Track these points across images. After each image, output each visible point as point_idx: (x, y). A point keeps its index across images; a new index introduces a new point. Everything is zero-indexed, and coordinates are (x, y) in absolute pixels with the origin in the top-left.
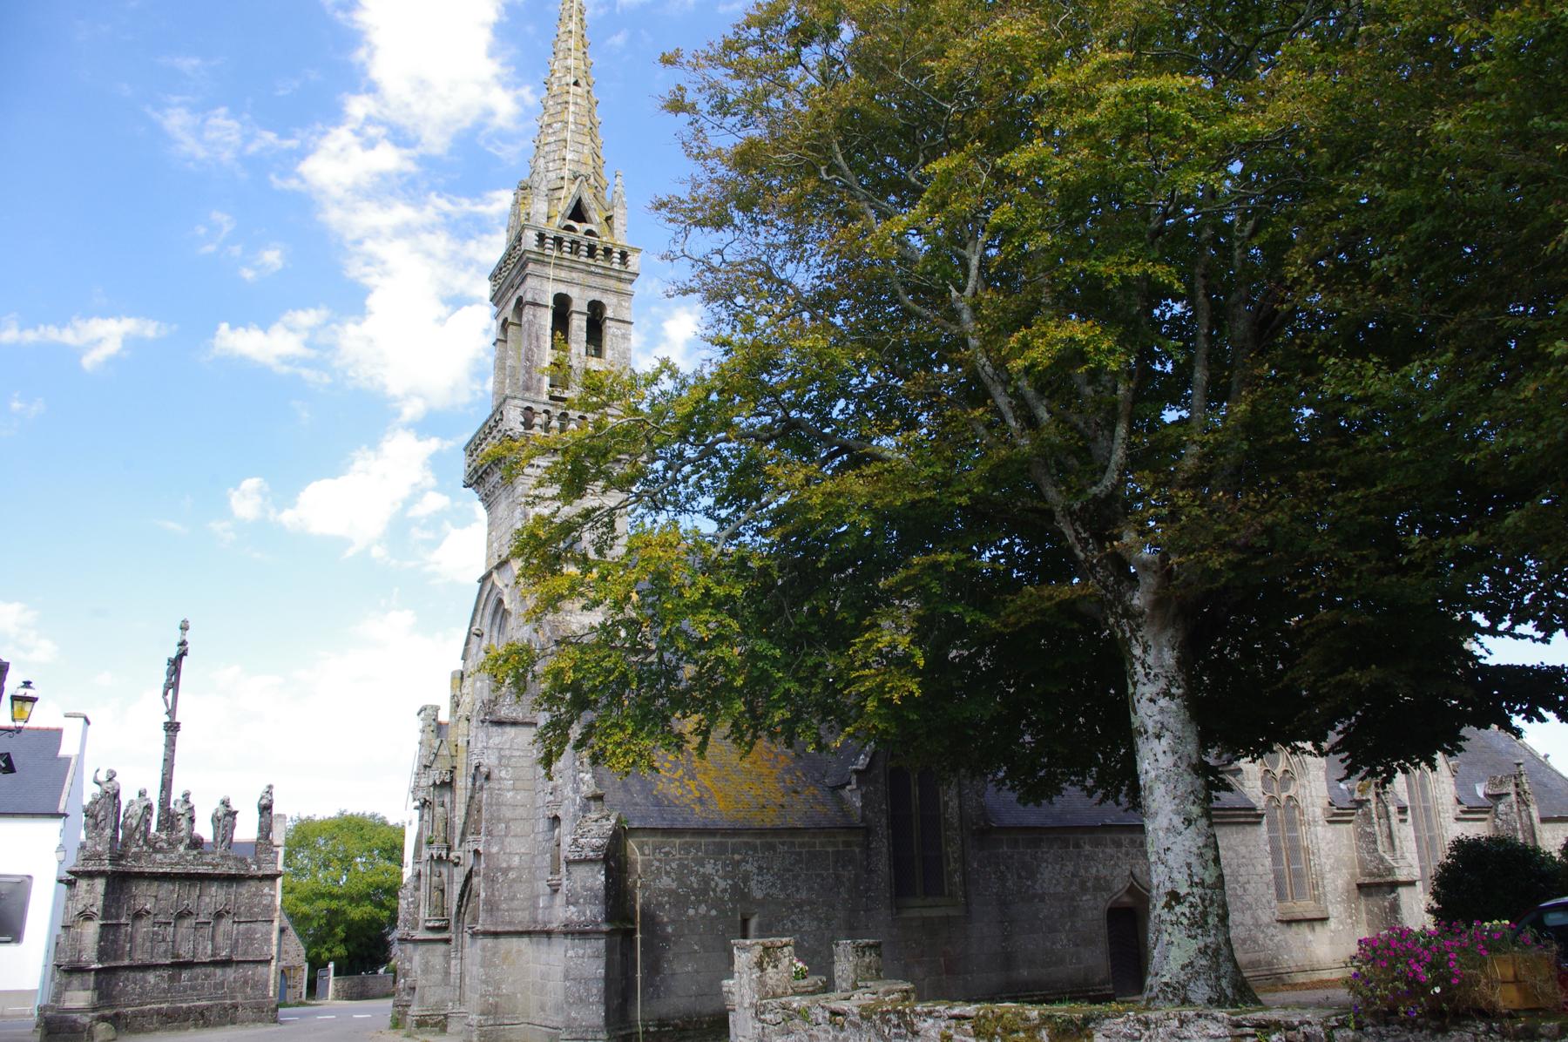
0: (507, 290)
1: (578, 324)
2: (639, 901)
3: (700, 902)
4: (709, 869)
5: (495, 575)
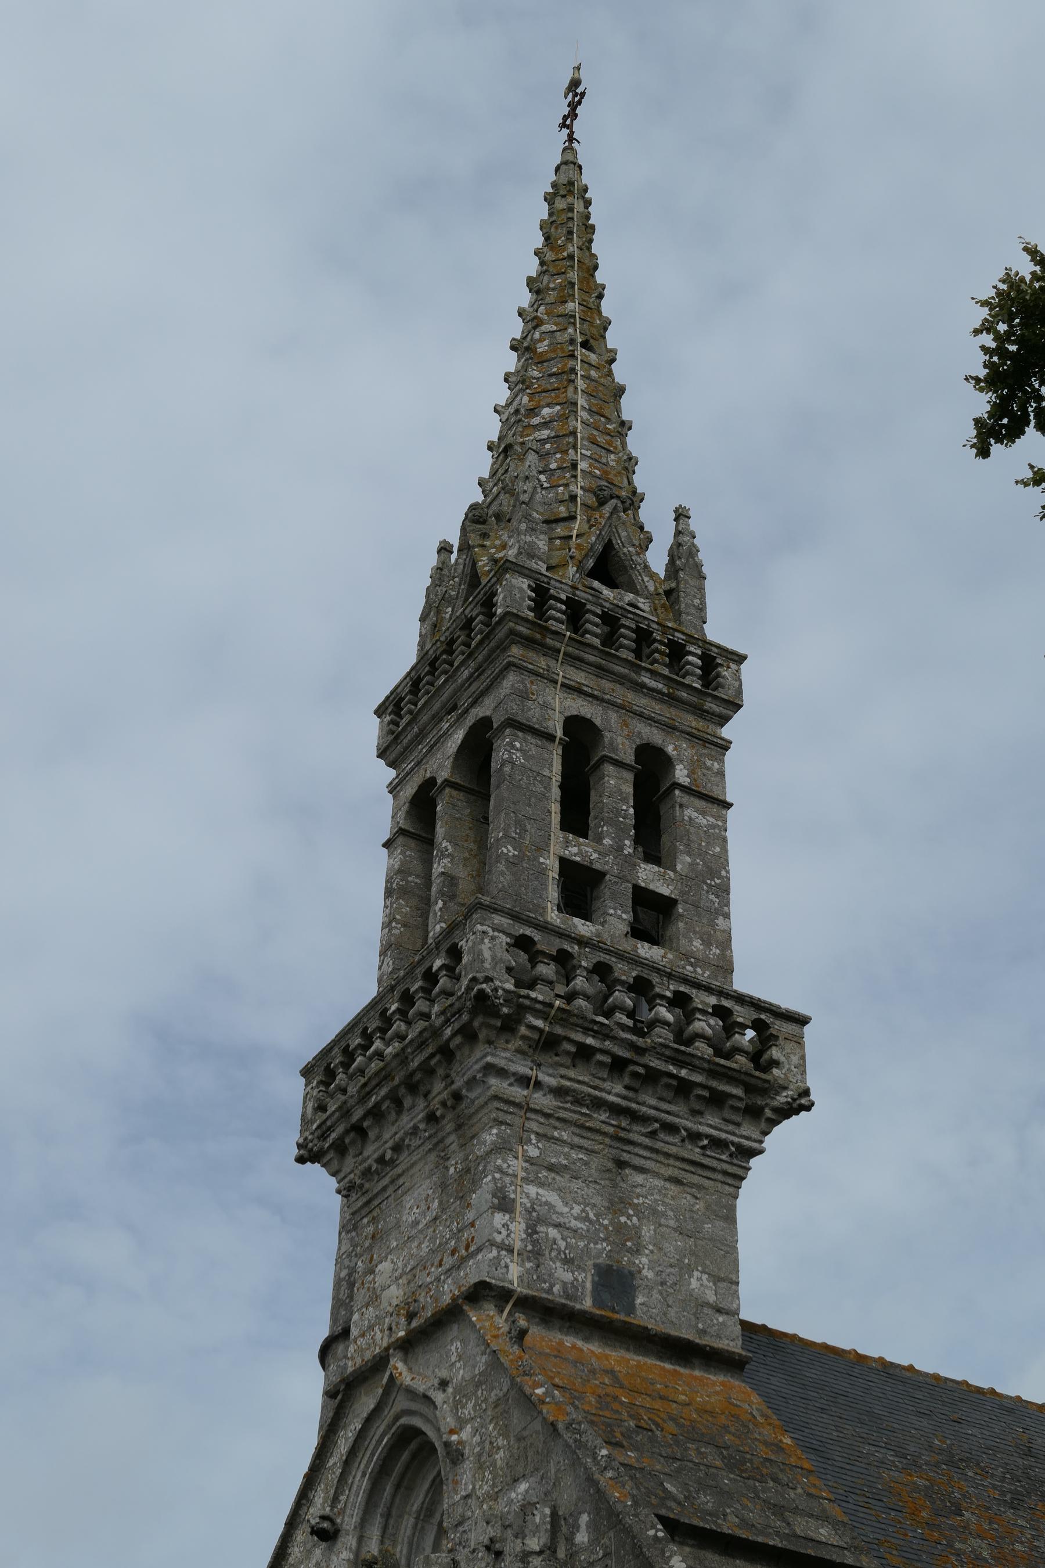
0: (437, 719)
1: (615, 789)
5: (398, 1365)
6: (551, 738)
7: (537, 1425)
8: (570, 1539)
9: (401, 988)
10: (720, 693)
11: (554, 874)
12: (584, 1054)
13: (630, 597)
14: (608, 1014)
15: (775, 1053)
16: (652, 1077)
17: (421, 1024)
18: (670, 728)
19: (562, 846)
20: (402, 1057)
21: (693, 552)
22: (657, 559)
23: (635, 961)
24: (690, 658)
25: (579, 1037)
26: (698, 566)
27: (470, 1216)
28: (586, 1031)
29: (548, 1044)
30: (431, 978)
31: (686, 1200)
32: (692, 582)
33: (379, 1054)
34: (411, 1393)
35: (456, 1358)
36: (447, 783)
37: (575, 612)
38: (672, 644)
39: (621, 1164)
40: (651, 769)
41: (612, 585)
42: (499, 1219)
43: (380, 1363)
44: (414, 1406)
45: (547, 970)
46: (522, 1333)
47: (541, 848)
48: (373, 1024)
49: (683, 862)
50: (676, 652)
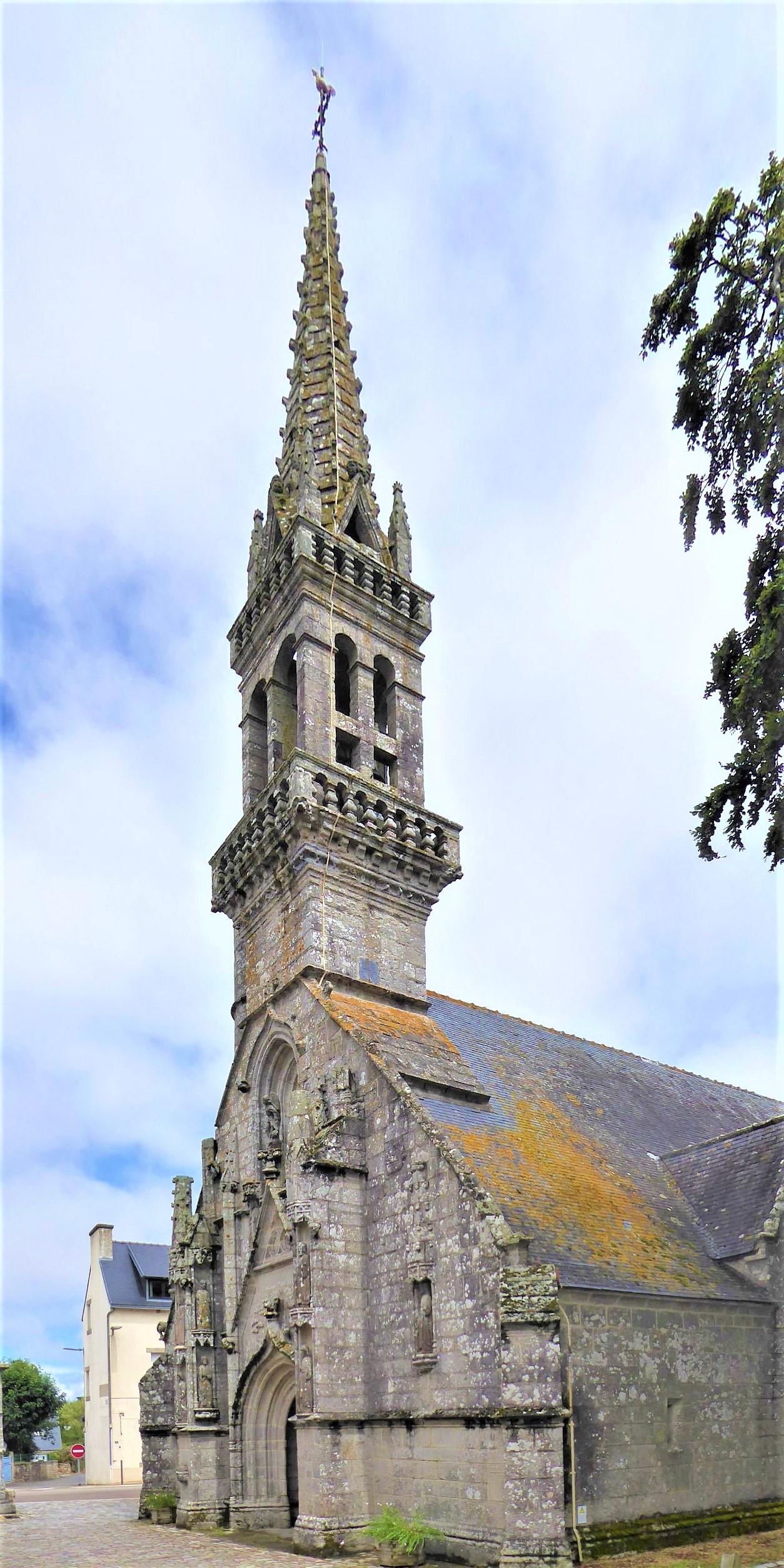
1: (364, 683)
6: (328, 648)
7: (339, 1033)
8: (356, 1084)
9: (257, 809)
12: (353, 844)
13: (368, 551)
14: (364, 822)
16: (385, 859)
17: (268, 830)
18: (392, 645)
19: (338, 721)
21: (405, 518)
22: (384, 522)
23: (378, 792)
24: (404, 596)
25: (350, 835)
26: (407, 529)
27: (301, 934)
29: (336, 839)
32: (405, 542)
33: (249, 849)
34: (279, 1023)
35: (299, 1003)
36: (273, 681)
37: (339, 554)
39: (371, 907)
41: (358, 540)
42: (315, 935)
44: (280, 1029)
45: (332, 795)
46: (330, 990)
47: (326, 721)
48: (244, 832)
49: (399, 733)
50: (396, 591)
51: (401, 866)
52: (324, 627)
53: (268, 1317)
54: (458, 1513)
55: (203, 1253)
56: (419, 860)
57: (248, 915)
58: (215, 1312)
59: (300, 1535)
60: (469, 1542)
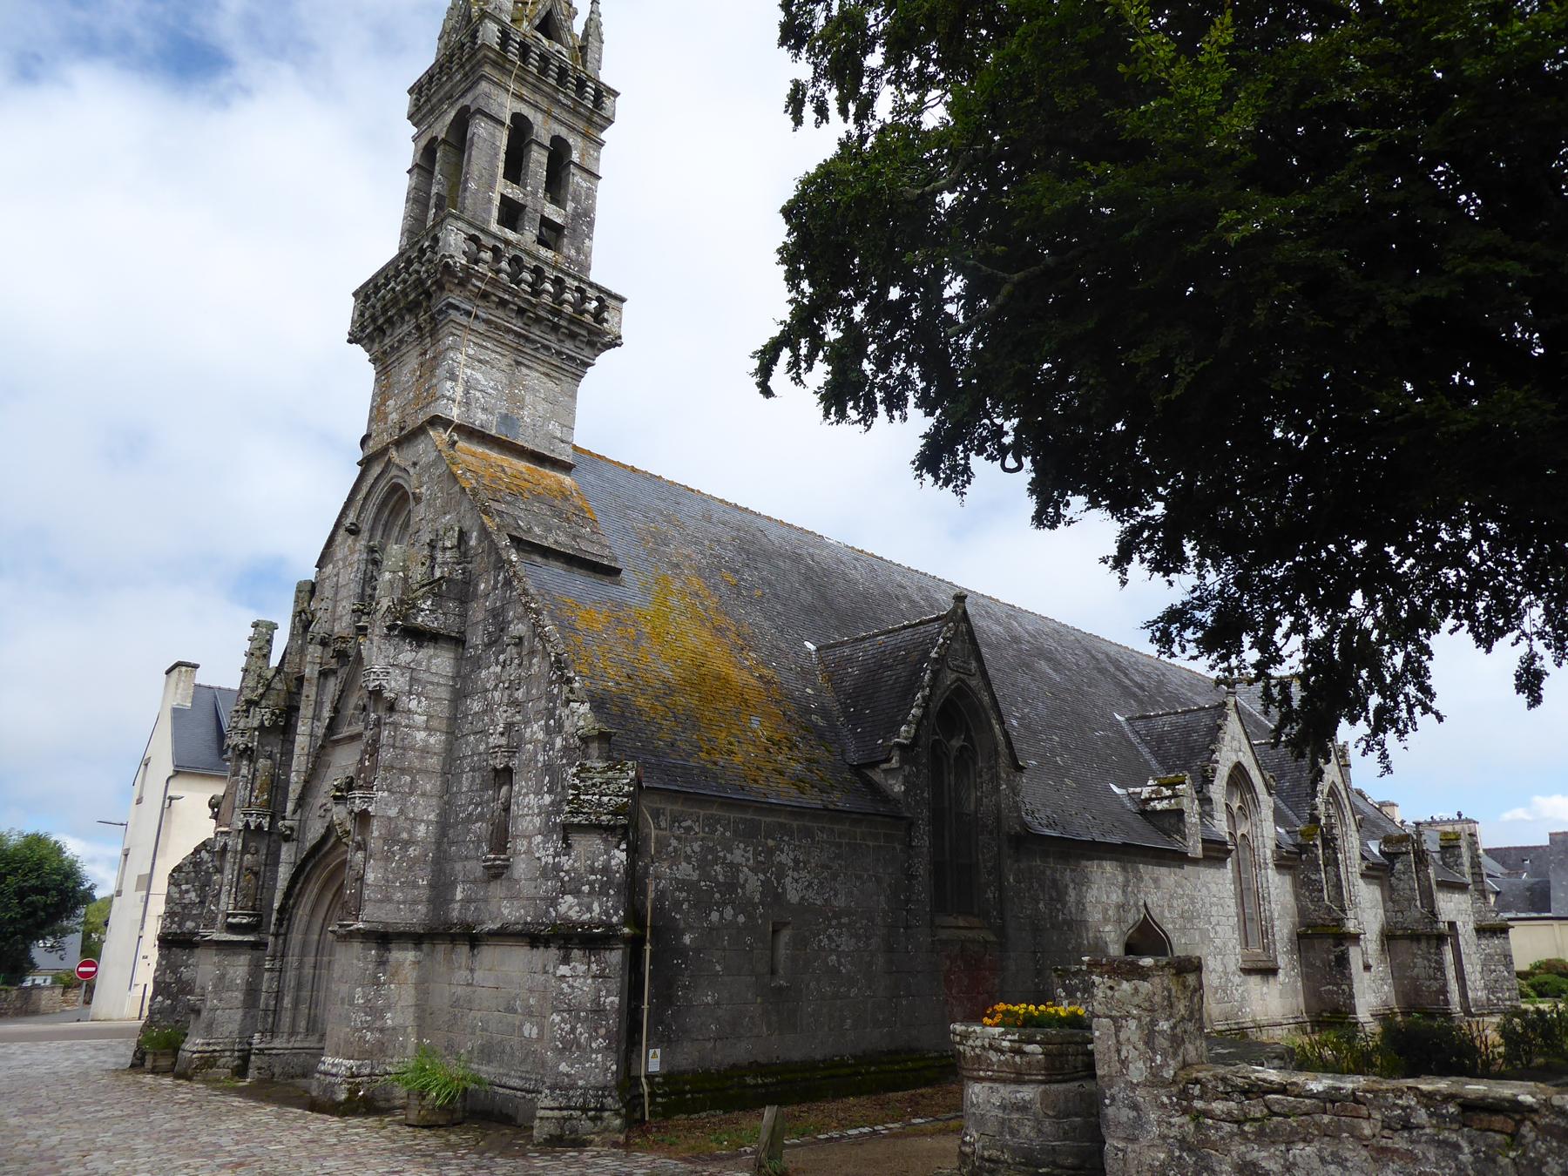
0: (441, 101)
1: (538, 159)
2: (651, 895)
3: (725, 904)
4: (737, 856)
5: (393, 453)
6: (503, 124)
10: (603, 113)
11: (497, 202)
12: (503, 303)
13: (558, 46)
14: (518, 284)
15: (606, 315)
17: (414, 276)
18: (572, 129)
19: (502, 187)
20: (404, 293)
21: (598, 26)
22: (578, 27)
23: (537, 258)
26: (600, 35)
27: (435, 381)
28: (505, 291)
29: (485, 296)
30: (422, 251)
31: (551, 385)
33: (393, 289)
35: (422, 450)
37: (525, 50)
38: (579, 79)
39: (518, 363)
40: (559, 153)
41: (549, 37)
42: (449, 384)
43: (385, 450)
45: (487, 256)
46: (455, 443)
47: (491, 187)
48: (391, 273)
49: (570, 206)
50: (581, 85)
51: (555, 328)
52: (501, 105)
53: (335, 797)
54: (512, 1055)
55: (273, 714)
56: (573, 326)
57: (384, 353)
58: (277, 787)
59: (320, 1084)
60: (519, 1094)
